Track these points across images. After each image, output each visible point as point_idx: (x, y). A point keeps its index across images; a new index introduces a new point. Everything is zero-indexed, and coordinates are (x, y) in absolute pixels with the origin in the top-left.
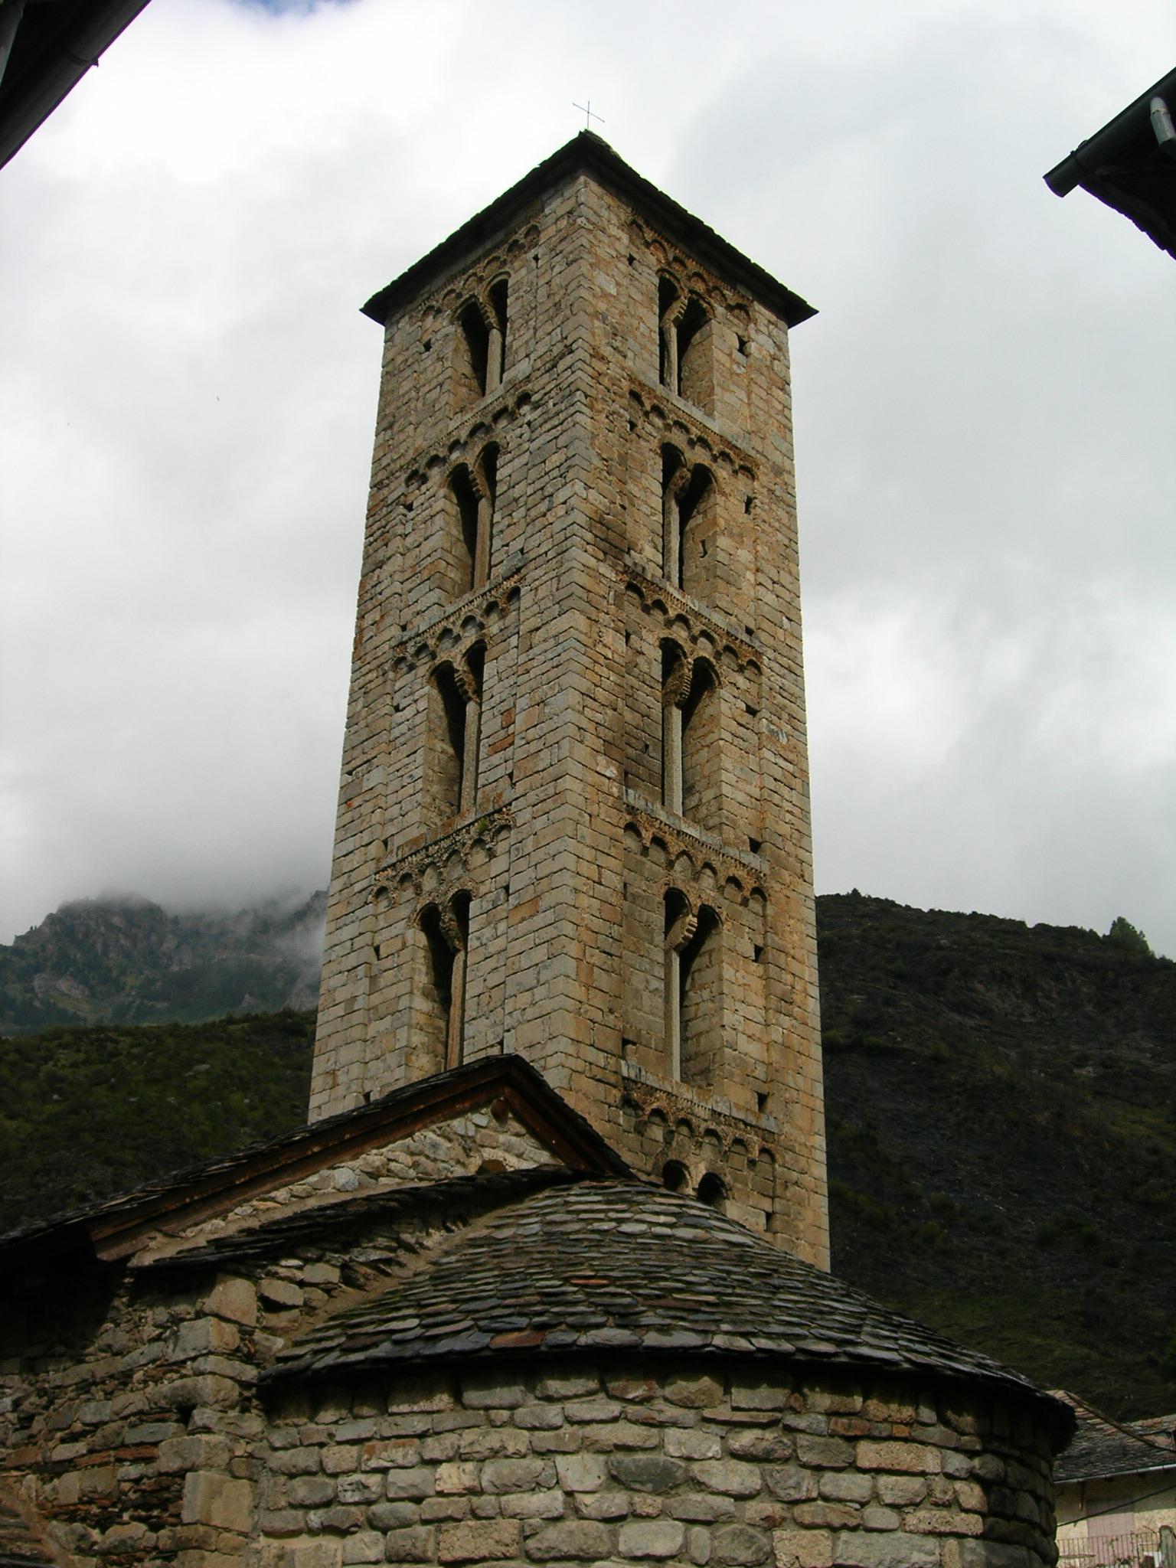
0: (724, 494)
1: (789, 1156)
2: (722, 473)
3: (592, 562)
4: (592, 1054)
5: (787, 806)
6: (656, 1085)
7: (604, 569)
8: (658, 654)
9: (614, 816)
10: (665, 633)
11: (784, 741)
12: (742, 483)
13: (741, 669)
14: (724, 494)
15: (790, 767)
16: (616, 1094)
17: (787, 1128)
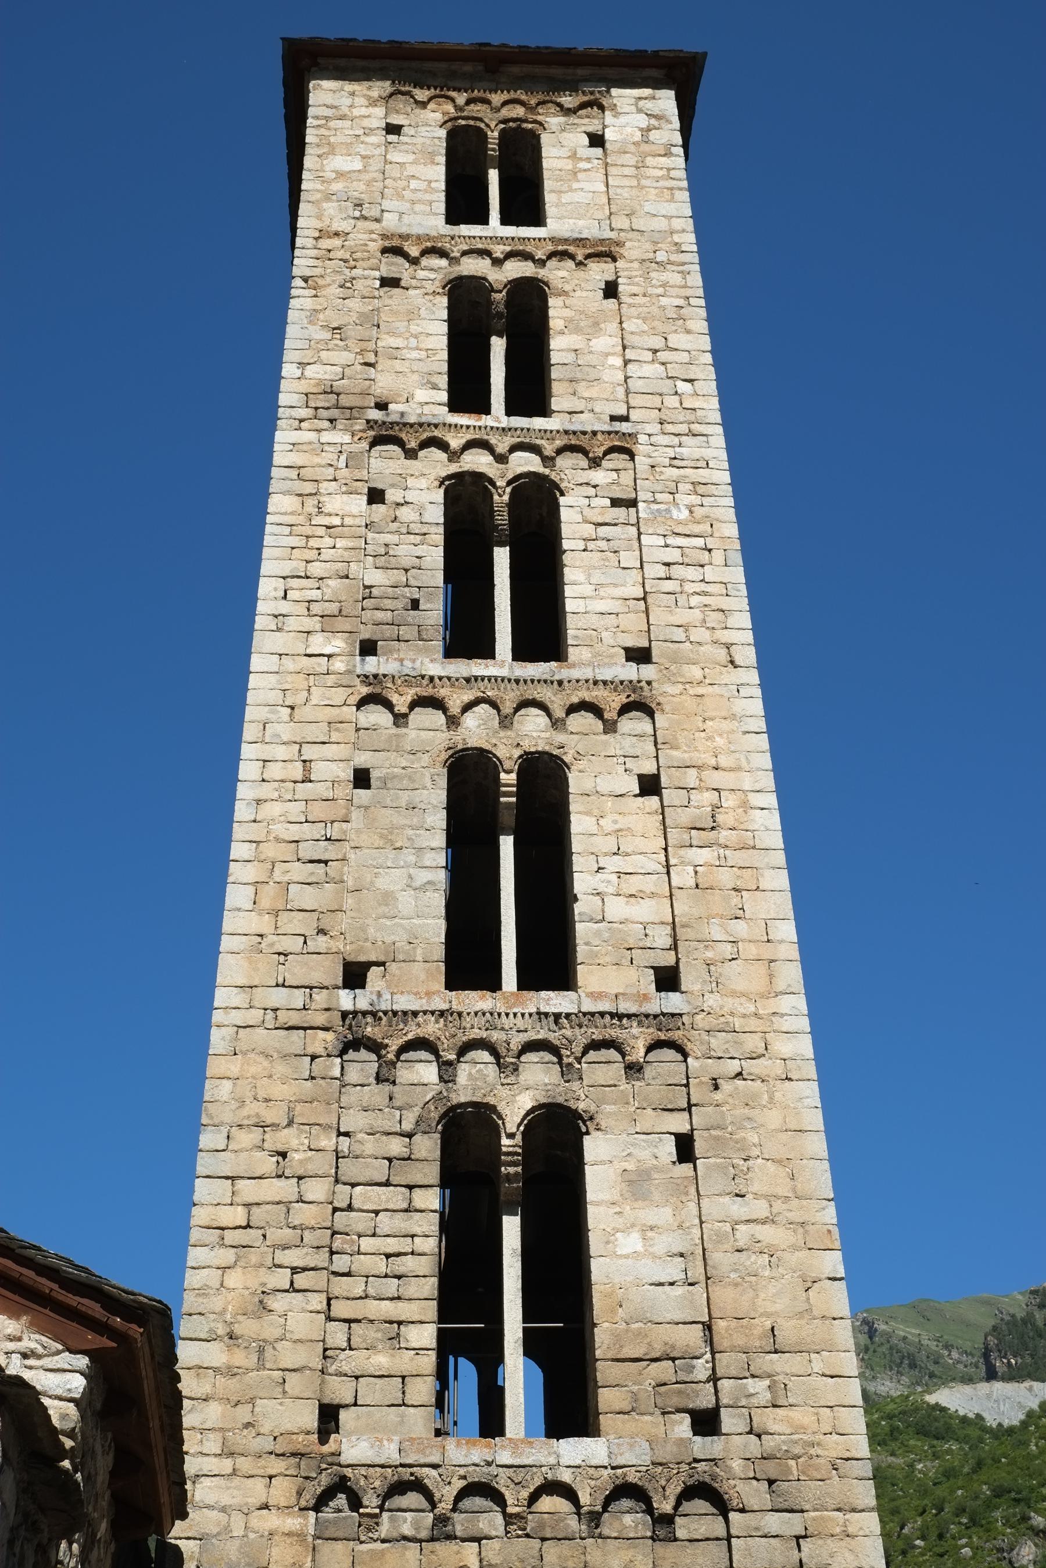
0: (565, 293)
1: (718, 1043)
2: (556, 273)
3: (312, 436)
4: (278, 997)
5: (689, 588)
6: (414, 1008)
7: (326, 437)
8: (439, 496)
9: (339, 695)
10: (454, 468)
11: (685, 514)
12: (599, 272)
13: (595, 463)
14: (565, 293)
15: (699, 542)
16: (323, 1041)
17: (712, 1001)
